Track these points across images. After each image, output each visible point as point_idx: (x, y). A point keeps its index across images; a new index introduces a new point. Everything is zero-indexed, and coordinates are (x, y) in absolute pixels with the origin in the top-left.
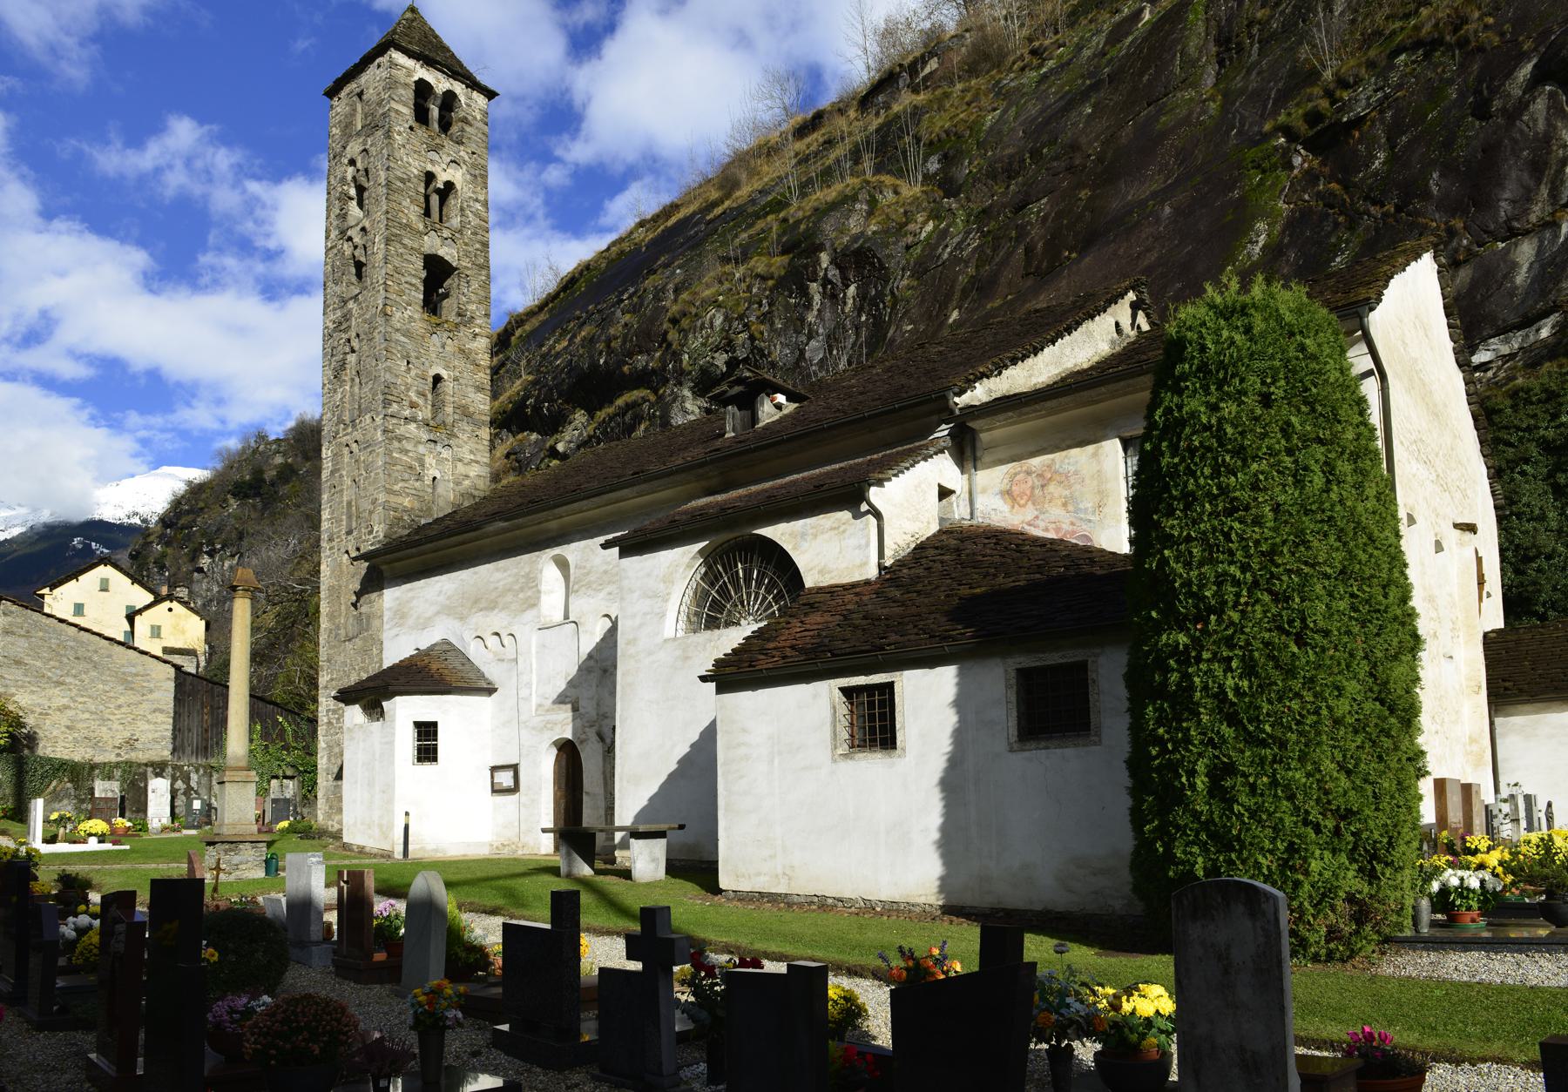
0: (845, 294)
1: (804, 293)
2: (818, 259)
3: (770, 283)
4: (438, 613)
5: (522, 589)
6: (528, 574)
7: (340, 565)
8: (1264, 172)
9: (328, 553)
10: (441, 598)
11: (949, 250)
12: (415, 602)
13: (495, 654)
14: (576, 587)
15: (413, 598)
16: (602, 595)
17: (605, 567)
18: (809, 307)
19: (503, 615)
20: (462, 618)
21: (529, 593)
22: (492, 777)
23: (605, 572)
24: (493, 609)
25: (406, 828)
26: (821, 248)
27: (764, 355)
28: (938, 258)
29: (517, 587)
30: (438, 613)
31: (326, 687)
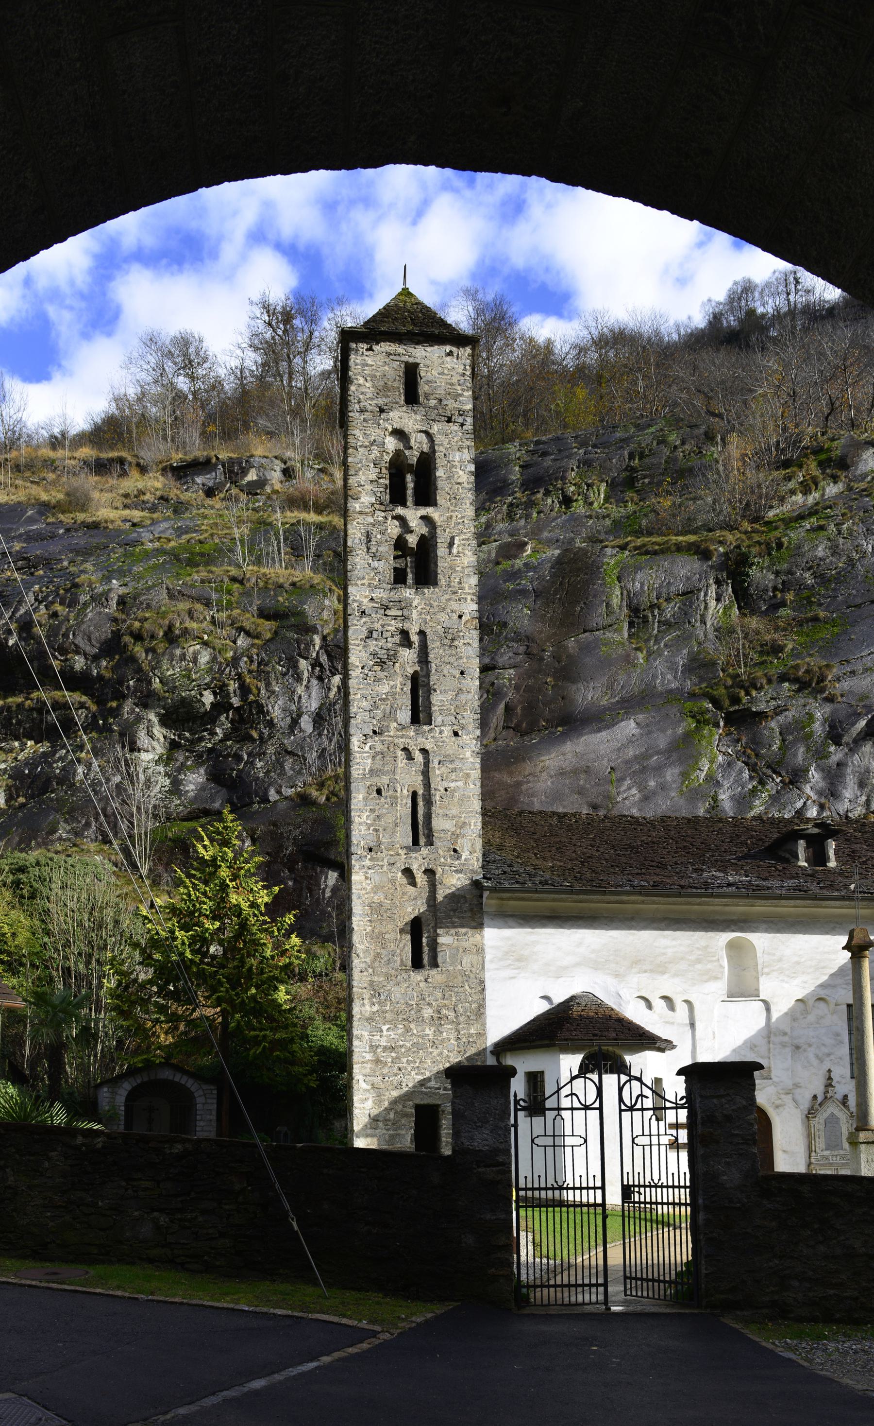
0: (329, 680)
1: (293, 665)
2: (312, 640)
3: (256, 641)
4: (577, 964)
5: (698, 961)
6: (706, 947)
7: (393, 881)
9: (367, 863)
14: (766, 970)
16: (796, 982)
17: (796, 959)
18: (299, 679)
20: (617, 976)
21: (709, 966)
23: (798, 963)
24: (663, 973)
26: (314, 630)
27: (263, 712)
29: (693, 958)
30: (577, 964)
31: (370, 1020)
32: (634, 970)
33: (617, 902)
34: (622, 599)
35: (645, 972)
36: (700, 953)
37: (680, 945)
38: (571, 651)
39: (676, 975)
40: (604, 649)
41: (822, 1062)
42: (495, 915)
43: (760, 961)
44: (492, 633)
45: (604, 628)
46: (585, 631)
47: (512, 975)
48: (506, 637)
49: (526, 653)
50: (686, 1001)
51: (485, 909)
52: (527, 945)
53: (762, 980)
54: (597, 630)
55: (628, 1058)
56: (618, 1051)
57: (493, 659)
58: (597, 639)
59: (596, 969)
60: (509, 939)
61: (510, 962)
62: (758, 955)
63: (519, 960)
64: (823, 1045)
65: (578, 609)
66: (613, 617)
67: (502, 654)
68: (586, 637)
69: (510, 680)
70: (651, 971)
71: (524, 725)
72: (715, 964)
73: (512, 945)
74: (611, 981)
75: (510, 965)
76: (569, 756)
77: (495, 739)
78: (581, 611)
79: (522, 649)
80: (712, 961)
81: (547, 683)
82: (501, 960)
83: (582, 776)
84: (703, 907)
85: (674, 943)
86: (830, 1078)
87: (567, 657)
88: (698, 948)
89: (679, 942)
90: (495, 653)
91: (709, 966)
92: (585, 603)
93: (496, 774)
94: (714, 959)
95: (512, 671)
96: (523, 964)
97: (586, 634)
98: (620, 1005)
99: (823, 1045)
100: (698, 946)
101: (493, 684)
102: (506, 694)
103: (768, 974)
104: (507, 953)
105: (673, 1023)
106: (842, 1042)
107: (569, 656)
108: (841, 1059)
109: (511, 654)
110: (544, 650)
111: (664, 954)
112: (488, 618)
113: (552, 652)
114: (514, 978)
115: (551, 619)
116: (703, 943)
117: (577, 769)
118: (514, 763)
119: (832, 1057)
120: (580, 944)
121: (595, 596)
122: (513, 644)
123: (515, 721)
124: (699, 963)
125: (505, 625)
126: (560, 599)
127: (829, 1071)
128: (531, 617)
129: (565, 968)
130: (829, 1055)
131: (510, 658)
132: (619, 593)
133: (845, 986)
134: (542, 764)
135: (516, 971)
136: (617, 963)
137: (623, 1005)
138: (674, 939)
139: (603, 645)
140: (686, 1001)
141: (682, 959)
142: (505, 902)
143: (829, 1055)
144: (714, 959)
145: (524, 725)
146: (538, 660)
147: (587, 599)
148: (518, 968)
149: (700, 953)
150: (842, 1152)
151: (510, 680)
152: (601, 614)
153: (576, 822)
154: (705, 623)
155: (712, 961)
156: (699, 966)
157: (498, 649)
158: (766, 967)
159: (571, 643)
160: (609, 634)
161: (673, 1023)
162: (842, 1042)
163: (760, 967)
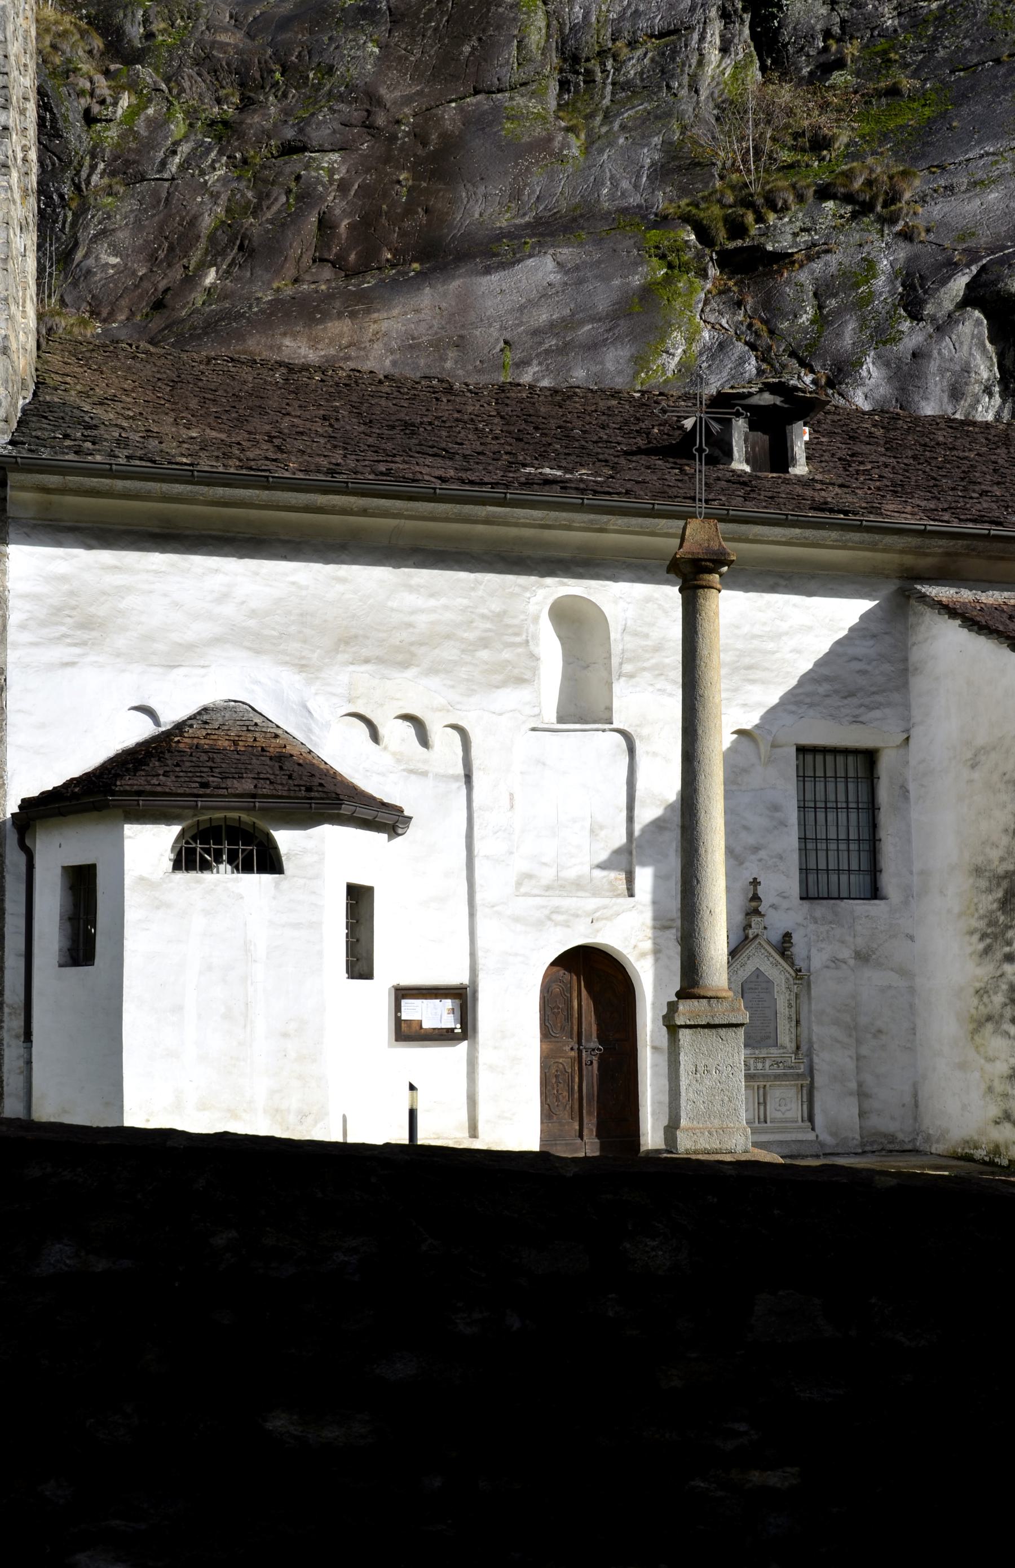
4: (217, 641)
5: (484, 643)
6: (501, 615)
8: (670, 266)
10: (228, 610)
11: (177, 160)
12: (130, 601)
13: (399, 757)
14: (627, 668)
15: (129, 589)
19: (434, 682)
21: (507, 655)
22: (398, 1008)
24: (405, 665)
25: (412, 1114)
28: (163, 164)
29: (471, 635)
30: (217, 641)
32: (341, 657)
33: (307, 509)
34: (549, 36)
35: (367, 661)
36: (489, 625)
37: (446, 608)
38: (448, 125)
39: (433, 670)
40: (508, 125)
41: (741, 863)
42: (35, 527)
43: (616, 649)
44: (306, 84)
45: (512, 89)
46: (477, 92)
47: (66, 660)
48: (330, 93)
49: (364, 125)
50: (455, 727)
51: (11, 511)
52: (104, 593)
53: (619, 688)
54: (500, 91)
55: (285, 839)
56: (261, 824)
57: (301, 131)
58: (497, 109)
59: (258, 652)
60: (63, 578)
61: (63, 629)
62: (613, 636)
63: (87, 624)
64: (746, 828)
65: (467, 49)
66: (530, 68)
67: (319, 124)
68: (478, 103)
69: (331, 172)
70: (380, 661)
71: (352, 257)
72: (520, 650)
73: (72, 593)
74: (290, 680)
75: (64, 636)
76: (426, 314)
77: (296, 281)
78: (471, 53)
79: (357, 116)
80: (513, 645)
81: (399, 182)
82: (43, 624)
83: (450, 355)
84: (495, 528)
85: (432, 602)
86: (756, 898)
87: (440, 136)
88: (483, 617)
89: (443, 601)
90: (307, 121)
91: (507, 655)
92: (480, 39)
93: (287, 341)
94: (518, 639)
95: (335, 156)
96: (95, 634)
97: (479, 97)
98: (310, 730)
99: (746, 828)
100: (486, 611)
101: (298, 178)
102: (322, 198)
103: (631, 676)
104: (57, 611)
105: (424, 774)
106: (783, 824)
107: (444, 136)
108: (781, 858)
109: (337, 126)
110: (398, 122)
111: (410, 625)
112: (299, 56)
113: (414, 125)
114: (72, 664)
115: (416, 67)
116: (495, 606)
117: (439, 340)
118: (321, 321)
119: (762, 854)
120: (223, 597)
121: (498, 27)
122: (341, 106)
123: (335, 250)
124: (486, 647)
125: (330, 70)
126: (436, 29)
127: (755, 883)
128: (378, 58)
129: (190, 647)
130: (756, 849)
131: (334, 132)
132: (543, 24)
133: (793, 708)
134: (374, 327)
135: (77, 650)
136: (305, 642)
137: (316, 729)
138: (432, 595)
139: (508, 118)
140: (455, 727)
141: (448, 637)
142: (55, 498)
143: (756, 849)
144: (518, 639)
145: (352, 257)
146: (387, 139)
147: (484, 30)
148: (84, 644)
149: (489, 625)
150: (774, 1051)
151: (331, 172)
152: (508, 62)
153: (322, 381)
154: (697, 92)
155: (513, 645)
156: (484, 654)
157: (313, 114)
158: (629, 660)
159: (450, 114)
160: (520, 101)
161: (424, 774)
162: (783, 824)
163: (615, 661)
